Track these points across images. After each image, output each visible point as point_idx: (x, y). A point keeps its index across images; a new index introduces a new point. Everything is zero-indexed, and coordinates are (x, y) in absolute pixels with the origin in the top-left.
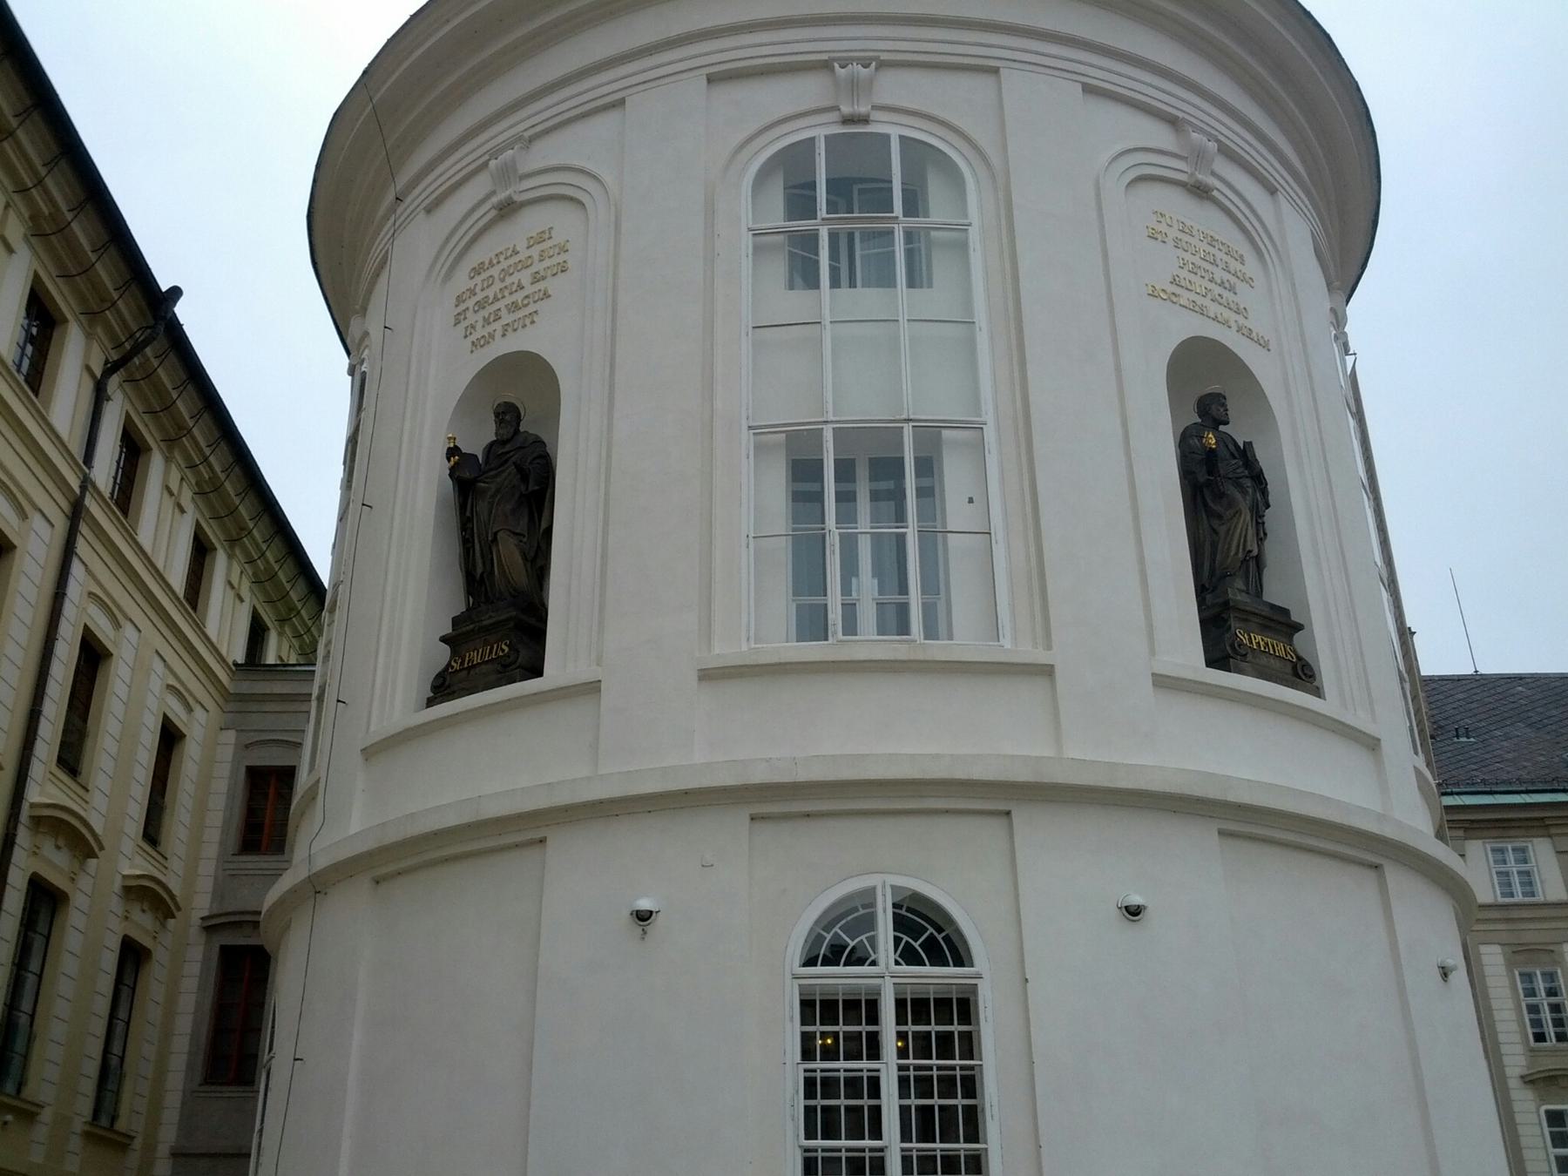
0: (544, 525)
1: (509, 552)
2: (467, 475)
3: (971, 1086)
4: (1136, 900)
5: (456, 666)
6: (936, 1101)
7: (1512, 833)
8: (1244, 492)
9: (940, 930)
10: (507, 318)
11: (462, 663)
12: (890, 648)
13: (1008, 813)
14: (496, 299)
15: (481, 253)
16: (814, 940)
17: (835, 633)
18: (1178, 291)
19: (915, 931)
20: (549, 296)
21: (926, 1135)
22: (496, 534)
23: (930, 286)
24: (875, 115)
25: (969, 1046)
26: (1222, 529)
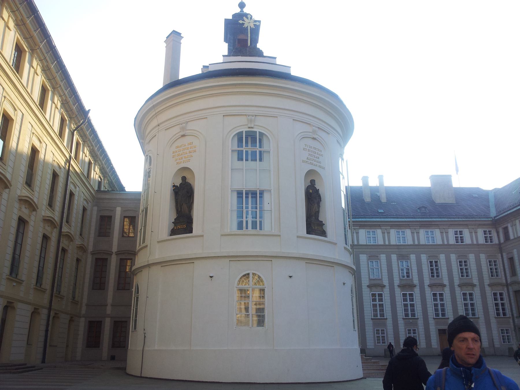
0: (191, 201)
5: (176, 228)
7: (402, 228)
11: (177, 228)
12: (254, 232)
14: (181, 155)
16: (239, 281)
17: (244, 229)
18: (308, 161)
20: (192, 157)
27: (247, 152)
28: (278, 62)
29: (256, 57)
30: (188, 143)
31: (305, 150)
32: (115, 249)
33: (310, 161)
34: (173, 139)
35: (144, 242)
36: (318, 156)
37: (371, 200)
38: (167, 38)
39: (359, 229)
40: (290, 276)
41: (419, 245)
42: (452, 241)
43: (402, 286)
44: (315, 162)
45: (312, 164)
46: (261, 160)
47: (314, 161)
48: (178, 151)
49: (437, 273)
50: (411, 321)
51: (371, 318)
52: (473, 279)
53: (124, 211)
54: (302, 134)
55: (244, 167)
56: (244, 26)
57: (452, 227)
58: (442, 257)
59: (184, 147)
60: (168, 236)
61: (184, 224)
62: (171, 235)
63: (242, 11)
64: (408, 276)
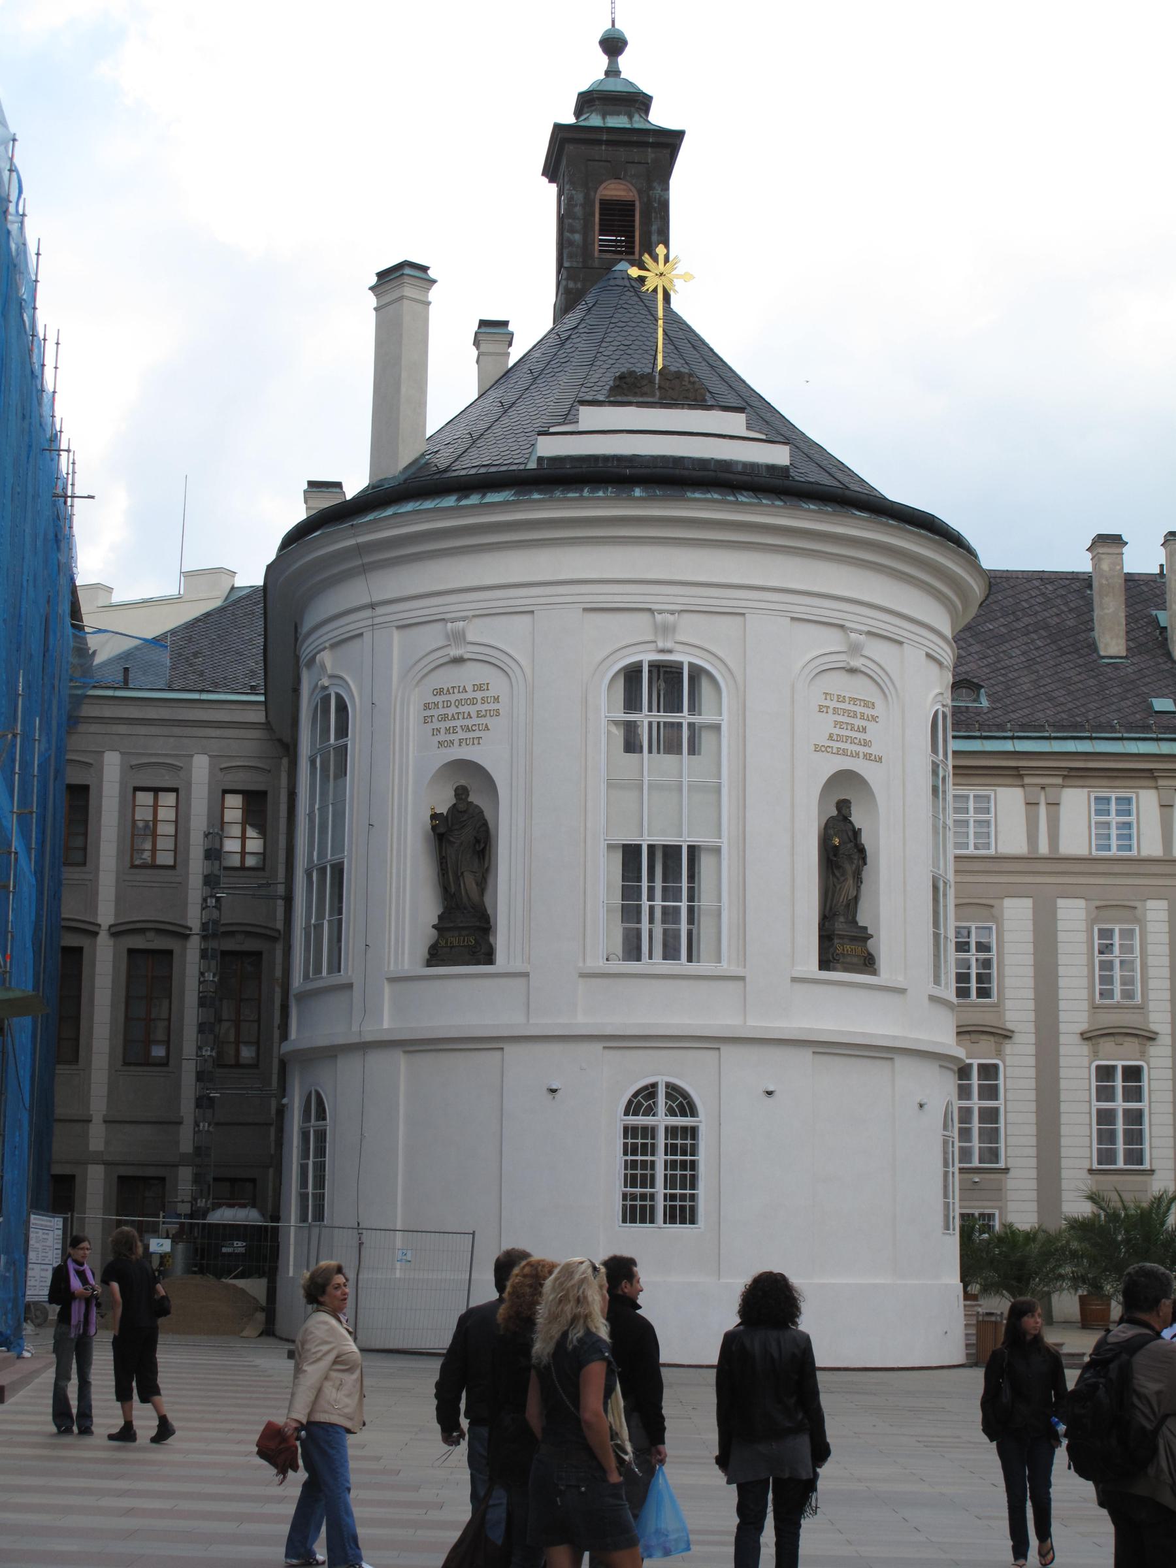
0: (486, 866)
1: (469, 881)
2: (442, 830)
3: (693, 1165)
4: (771, 1089)
5: (443, 943)
9: (685, 1098)
10: (462, 735)
11: (446, 943)
12: (669, 967)
13: (719, 1049)
16: (630, 1102)
19: (674, 1099)
21: (673, 1187)
22: (462, 873)
23: (699, 754)
24: (678, 647)
25: (694, 1151)
26: (838, 887)
29: (683, 408)
31: (825, 709)
32: (106, 915)
33: (836, 745)
34: (424, 662)
35: (335, 966)
36: (863, 723)
38: (381, 275)
39: (1063, 786)
40: (767, 1092)
44: (853, 745)
45: (844, 753)
46: (693, 751)
48: (440, 705)
51: (1088, 1167)
56: (644, 289)
59: (463, 696)
62: (429, 963)
63: (612, 72)
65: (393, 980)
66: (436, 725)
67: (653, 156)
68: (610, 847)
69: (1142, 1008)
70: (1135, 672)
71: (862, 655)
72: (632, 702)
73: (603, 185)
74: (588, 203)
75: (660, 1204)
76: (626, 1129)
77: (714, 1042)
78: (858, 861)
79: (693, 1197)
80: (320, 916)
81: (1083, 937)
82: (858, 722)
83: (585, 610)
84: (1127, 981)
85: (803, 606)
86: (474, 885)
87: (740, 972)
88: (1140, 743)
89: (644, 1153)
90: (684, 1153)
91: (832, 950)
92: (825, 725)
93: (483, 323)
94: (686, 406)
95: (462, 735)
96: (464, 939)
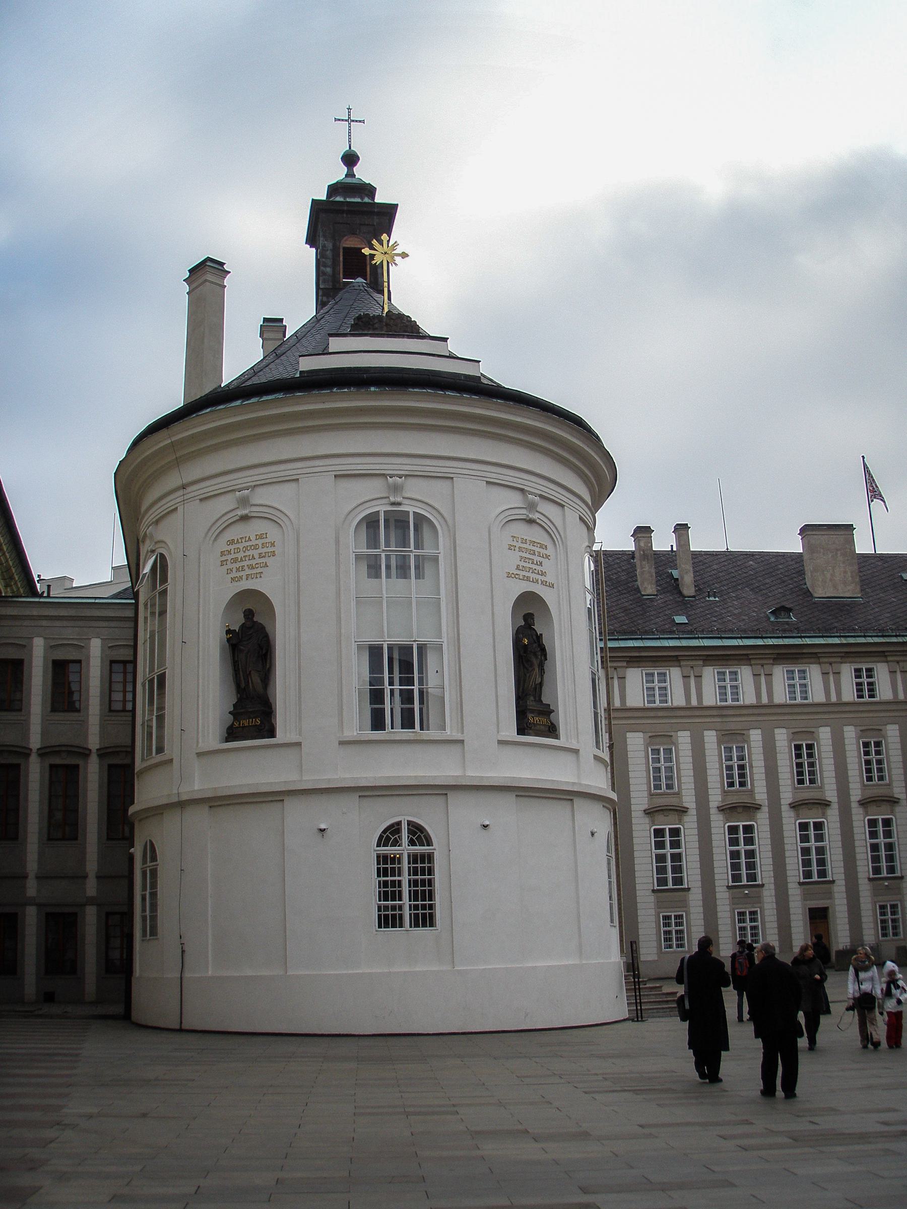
0: (268, 667)
1: (256, 678)
2: (234, 642)
3: (430, 883)
4: (487, 823)
5: (236, 724)
6: (419, 888)
7: (730, 663)
8: (537, 658)
9: (422, 833)
10: (248, 572)
11: (240, 724)
12: (407, 734)
13: (446, 794)
14: (242, 560)
15: (231, 534)
16: (381, 837)
17: (388, 728)
21: (416, 899)
23: (423, 579)
25: (430, 871)
26: (528, 675)
27: (388, 558)
28: (452, 347)
29: (403, 338)
30: (256, 535)
31: (512, 548)
32: (35, 741)
33: (522, 573)
34: (220, 522)
35: (160, 750)
37: (658, 591)
38: (190, 271)
41: (771, 706)
42: (849, 694)
43: (728, 810)
45: (528, 579)
47: (531, 571)
48: (232, 552)
49: (812, 773)
50: (747, 892)
52: (894, 784)
53: (51, 647)
54: (508, 513)
55: (384, 592)
56: (374, 262)
57: (850, 659)
58: (825, 734)
60: (220, 743)
61: (255, 718)
62: (227, 740)
63: (350, 174)
64: (742, 784)
65: (199, 755)
66: (230, 566)
67: (378, 220)
68: (360, 647)
69: (678, 794)
70: (662, 603)
71: (537, 511)
72: (373, 542)
73: (345, 238)
74: (335, 249)
75: (407, 913)
76: (378, 857)
77: (443, 790)
78: (541, 656)
79: (431, 907)
80: (151, 711)
81: (643, 754)
82: (536, 558)
83: (335, 476)
84: (669, 778)
85: (494, 474)
86: (259, 681)
87: (459, 736)
88: (669, 641)
89: (393, 875)
90: (423, 874)
91: (526, 720)
92: (513, 560)
93: (265, 320)
94: (406, 336)
95: (248, 572)
96: (252, 720)
